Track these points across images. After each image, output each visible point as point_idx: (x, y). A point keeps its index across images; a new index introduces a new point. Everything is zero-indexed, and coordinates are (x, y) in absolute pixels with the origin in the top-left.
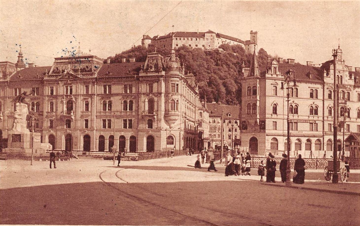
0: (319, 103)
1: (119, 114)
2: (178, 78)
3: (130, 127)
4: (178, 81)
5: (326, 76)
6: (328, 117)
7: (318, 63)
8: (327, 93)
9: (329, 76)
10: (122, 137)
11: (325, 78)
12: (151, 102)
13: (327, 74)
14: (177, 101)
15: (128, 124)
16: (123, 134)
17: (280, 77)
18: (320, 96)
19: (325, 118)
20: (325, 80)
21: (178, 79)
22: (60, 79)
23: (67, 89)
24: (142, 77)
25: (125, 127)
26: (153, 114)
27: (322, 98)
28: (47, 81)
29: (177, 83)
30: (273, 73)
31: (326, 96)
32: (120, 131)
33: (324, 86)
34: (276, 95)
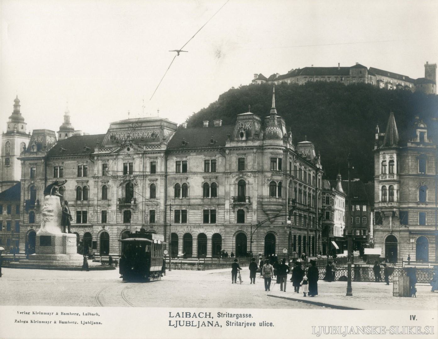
1: (199, 201)
2: (280, 149)
3: (214, 220)
10: (202, 237)
12: (242, 185)
14: (280, 183)
15: (210, 217)
16: (201, 231)
22: (116, 152)
23: (125, 168)
24: (230, 149)
25: (206, 220)
26: (245, 201)
28: (98, 155)
32: (199, 226)
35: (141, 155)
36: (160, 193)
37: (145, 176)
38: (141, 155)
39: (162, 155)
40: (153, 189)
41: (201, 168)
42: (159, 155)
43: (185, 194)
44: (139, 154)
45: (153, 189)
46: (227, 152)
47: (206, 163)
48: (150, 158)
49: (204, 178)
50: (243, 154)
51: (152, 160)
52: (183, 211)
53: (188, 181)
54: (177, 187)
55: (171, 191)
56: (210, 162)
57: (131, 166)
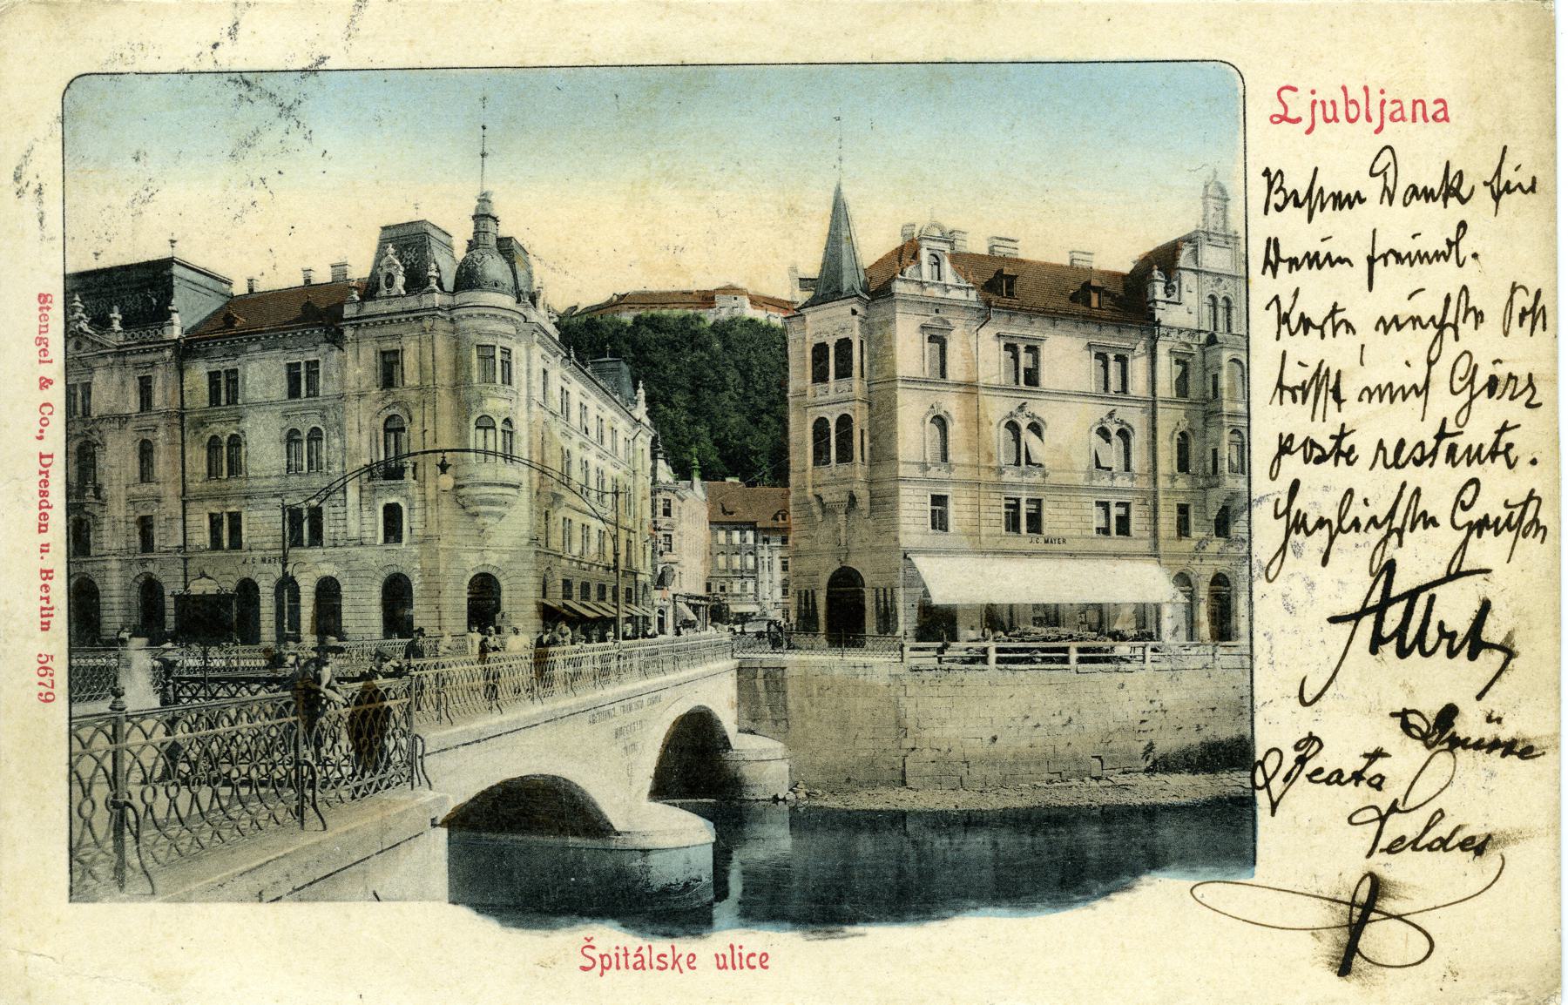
0: (1135, 418)
4: (505, 335)
5: (1164, 297)
6: (1173, 478)
7: (1117, 257)
8: (1167, 372)
9: (1174, 298)
11: (1160, 305)
13: (1169, 289)
17: (961, 295)
18: (1138, 385)
19: (1163, 483)
20: (1158, 314)
21: (510, 329)
27: (1146, 394)
29: (506, 343)
30: (926, 277)
31: (1165, 387)
33: (1154, 339)
34: (943, 374)
35: (110, 360)
36: (163, 463)
37: (123, 419)
38: (110, 360)
39: (168, 353)
40: (146, 451)
41: (280, 388)
42: (160, 355)
43: (235, 468)
44: (103, 356)
45: (146, 451)
46: (349, 333)
47: (292, 370)
48: (136, 366)
49: (285, 416)
50: (393, 337)
51: (142, 373)
52: (230, 514)
53: (242, 425)
54: (213, 445)
55: (197, 458)
56: (303, 369)
57: (87, 388)
